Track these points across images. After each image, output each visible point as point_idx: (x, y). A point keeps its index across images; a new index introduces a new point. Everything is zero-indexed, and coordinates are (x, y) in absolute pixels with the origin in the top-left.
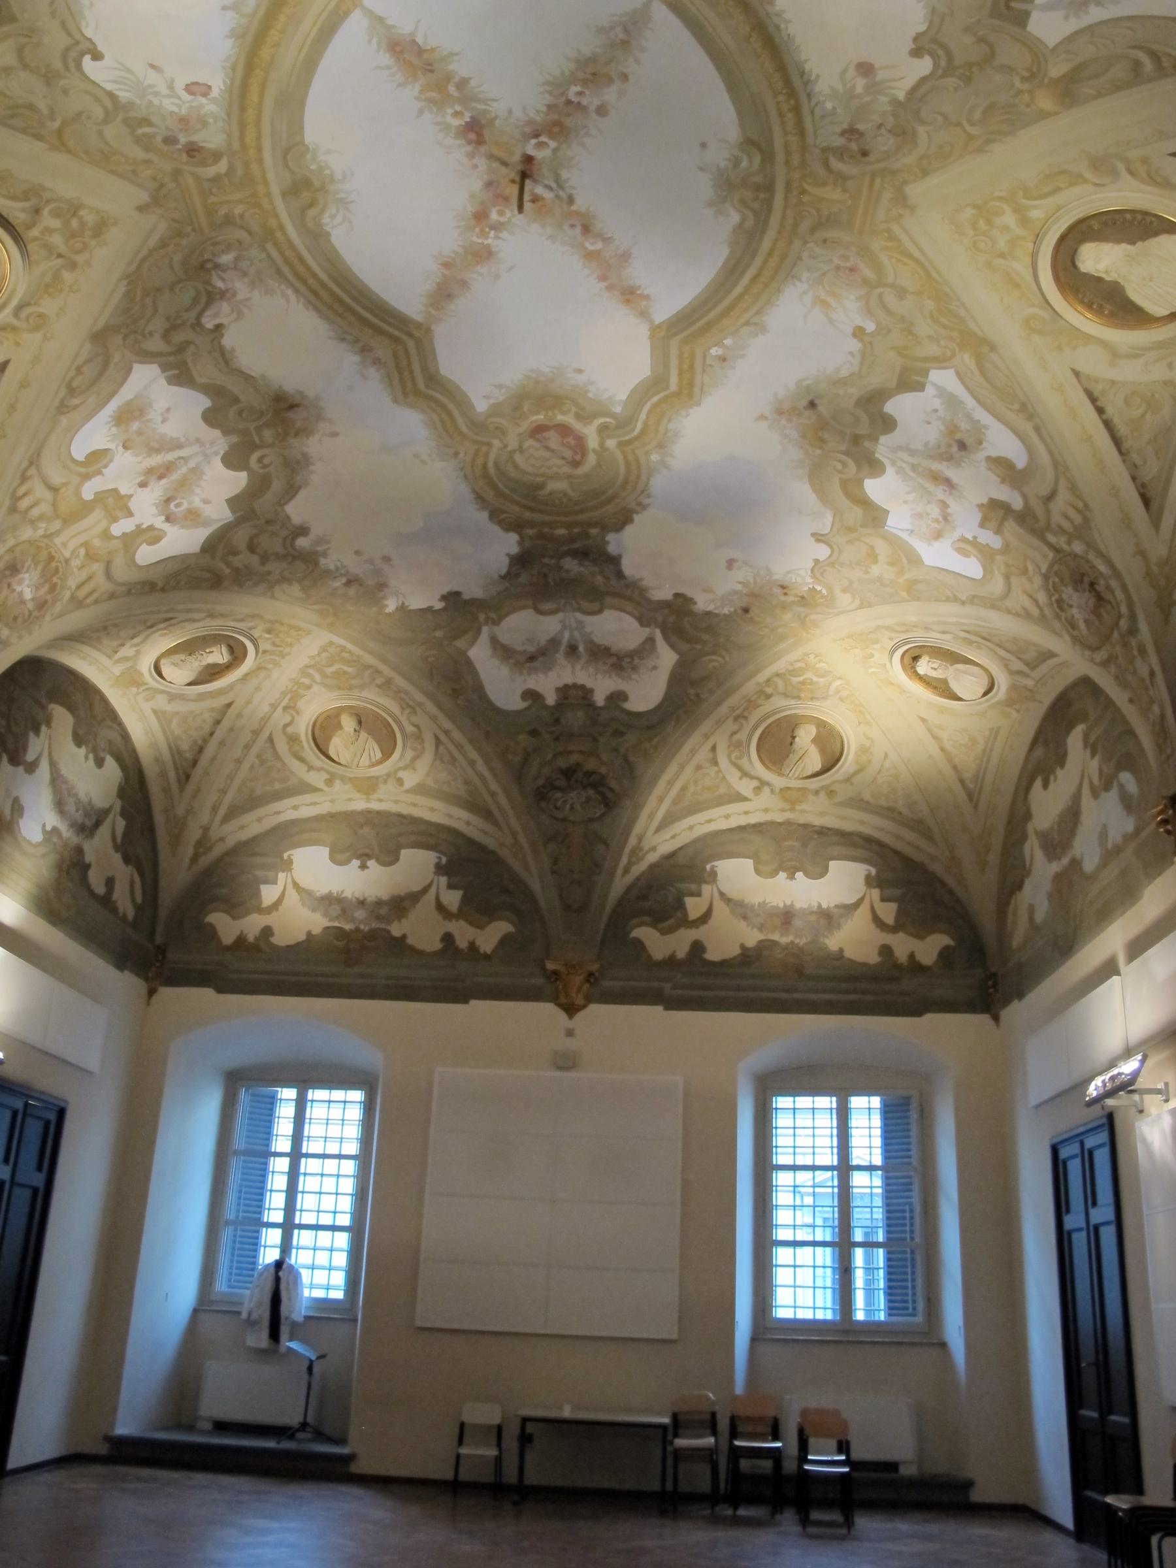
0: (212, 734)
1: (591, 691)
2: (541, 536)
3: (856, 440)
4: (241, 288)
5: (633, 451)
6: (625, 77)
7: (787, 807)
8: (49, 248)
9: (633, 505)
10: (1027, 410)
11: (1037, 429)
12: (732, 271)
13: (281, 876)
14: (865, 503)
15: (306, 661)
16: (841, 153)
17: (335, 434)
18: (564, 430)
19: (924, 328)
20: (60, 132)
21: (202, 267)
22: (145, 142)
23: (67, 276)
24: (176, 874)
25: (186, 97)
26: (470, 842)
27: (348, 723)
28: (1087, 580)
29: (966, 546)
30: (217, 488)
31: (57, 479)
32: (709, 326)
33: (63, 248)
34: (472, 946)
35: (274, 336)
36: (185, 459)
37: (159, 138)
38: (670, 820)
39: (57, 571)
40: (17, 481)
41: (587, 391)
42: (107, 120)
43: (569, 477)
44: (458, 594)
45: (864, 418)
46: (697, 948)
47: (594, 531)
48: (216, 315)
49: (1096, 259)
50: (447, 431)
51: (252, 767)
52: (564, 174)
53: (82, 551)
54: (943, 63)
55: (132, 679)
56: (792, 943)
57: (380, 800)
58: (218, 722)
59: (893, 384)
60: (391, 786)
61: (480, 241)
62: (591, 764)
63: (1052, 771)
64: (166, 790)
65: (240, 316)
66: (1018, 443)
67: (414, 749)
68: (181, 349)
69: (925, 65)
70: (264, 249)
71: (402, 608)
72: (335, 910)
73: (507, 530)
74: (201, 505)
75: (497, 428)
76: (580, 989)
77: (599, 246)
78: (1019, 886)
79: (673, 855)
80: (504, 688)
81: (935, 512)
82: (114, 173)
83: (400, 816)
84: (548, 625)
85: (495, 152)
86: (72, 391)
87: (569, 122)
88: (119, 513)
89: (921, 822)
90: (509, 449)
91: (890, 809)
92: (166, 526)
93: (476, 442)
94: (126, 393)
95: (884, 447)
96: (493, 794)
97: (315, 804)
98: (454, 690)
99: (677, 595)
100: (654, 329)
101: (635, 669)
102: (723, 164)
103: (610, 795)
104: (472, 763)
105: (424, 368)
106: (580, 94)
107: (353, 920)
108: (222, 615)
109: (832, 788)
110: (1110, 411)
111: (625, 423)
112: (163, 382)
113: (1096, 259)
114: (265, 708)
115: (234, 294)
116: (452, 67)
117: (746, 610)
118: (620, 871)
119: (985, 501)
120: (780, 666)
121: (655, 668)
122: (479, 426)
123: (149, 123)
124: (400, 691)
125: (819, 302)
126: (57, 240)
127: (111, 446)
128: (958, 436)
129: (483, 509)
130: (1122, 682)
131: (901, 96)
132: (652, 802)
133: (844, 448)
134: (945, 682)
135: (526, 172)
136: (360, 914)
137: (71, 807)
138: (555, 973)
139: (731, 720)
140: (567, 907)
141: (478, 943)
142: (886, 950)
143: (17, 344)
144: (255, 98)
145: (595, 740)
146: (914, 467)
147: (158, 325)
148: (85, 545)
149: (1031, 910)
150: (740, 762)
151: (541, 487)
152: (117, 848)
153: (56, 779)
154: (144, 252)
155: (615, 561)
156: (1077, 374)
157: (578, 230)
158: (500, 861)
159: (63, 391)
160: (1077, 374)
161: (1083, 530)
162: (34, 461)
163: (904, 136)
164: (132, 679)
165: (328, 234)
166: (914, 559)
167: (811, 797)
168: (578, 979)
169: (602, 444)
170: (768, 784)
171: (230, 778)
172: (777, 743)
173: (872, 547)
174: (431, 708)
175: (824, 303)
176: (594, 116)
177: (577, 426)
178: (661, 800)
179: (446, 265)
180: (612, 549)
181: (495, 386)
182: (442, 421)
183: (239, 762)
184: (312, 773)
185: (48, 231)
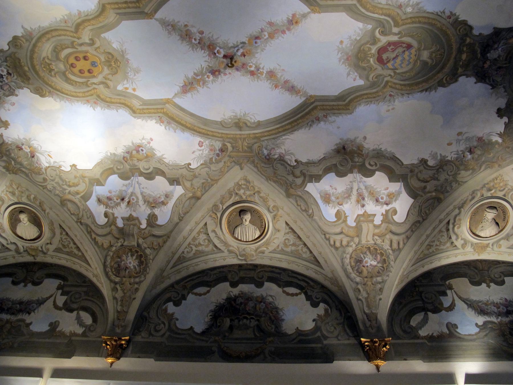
2: (466, 66)
5: (402, 20)
6: (186, 26)
8: (250, 196)
17: (365, 138)
18: (382, 50)
20: (212, 180)
21: (268, 159)
22: (217, 162)
25: (203, 148)
31: (338, 230)
33: (252, 192)
35: (305, 145)
39: (376, 249)
40: (327, 242)
41: (356, 39)
42: (210, 168)
47: (468, 40)
48: (290, 161)
50: (374, 97)
52: (231, 45)
61: (264, 75)
68: (304, 175)
70: (263, 141)
71: (500, 135)
73: (456, 81)
74: (388, 191)
75: (376, 78)
77: (266, 33)
82: (227, 172)
86: (306, 211)
87: (208, 43)
88: (371, 218)
90: (392, 74)
93: (385, 86)
100: (314, 11)
105: (333, 101)
106: (195, 40)
111: (380, 23)
112: (317, 184)
115: (282, 153)
116: (190, 77)
122: (373, 85)
123: (212, 158)
126: (248, 193)
143: (281, 217)
144: (204, 131)
147: (291, 178)
148: (374, 235)
154: (259, 173)
157: (258, 41)
165: (259, 121)
169: (396, 34)
176: (204, 35)
177: (379, 45)
179: (276, 87)
181: (348, 76)
182: (366, 98)
185: (244, 194)
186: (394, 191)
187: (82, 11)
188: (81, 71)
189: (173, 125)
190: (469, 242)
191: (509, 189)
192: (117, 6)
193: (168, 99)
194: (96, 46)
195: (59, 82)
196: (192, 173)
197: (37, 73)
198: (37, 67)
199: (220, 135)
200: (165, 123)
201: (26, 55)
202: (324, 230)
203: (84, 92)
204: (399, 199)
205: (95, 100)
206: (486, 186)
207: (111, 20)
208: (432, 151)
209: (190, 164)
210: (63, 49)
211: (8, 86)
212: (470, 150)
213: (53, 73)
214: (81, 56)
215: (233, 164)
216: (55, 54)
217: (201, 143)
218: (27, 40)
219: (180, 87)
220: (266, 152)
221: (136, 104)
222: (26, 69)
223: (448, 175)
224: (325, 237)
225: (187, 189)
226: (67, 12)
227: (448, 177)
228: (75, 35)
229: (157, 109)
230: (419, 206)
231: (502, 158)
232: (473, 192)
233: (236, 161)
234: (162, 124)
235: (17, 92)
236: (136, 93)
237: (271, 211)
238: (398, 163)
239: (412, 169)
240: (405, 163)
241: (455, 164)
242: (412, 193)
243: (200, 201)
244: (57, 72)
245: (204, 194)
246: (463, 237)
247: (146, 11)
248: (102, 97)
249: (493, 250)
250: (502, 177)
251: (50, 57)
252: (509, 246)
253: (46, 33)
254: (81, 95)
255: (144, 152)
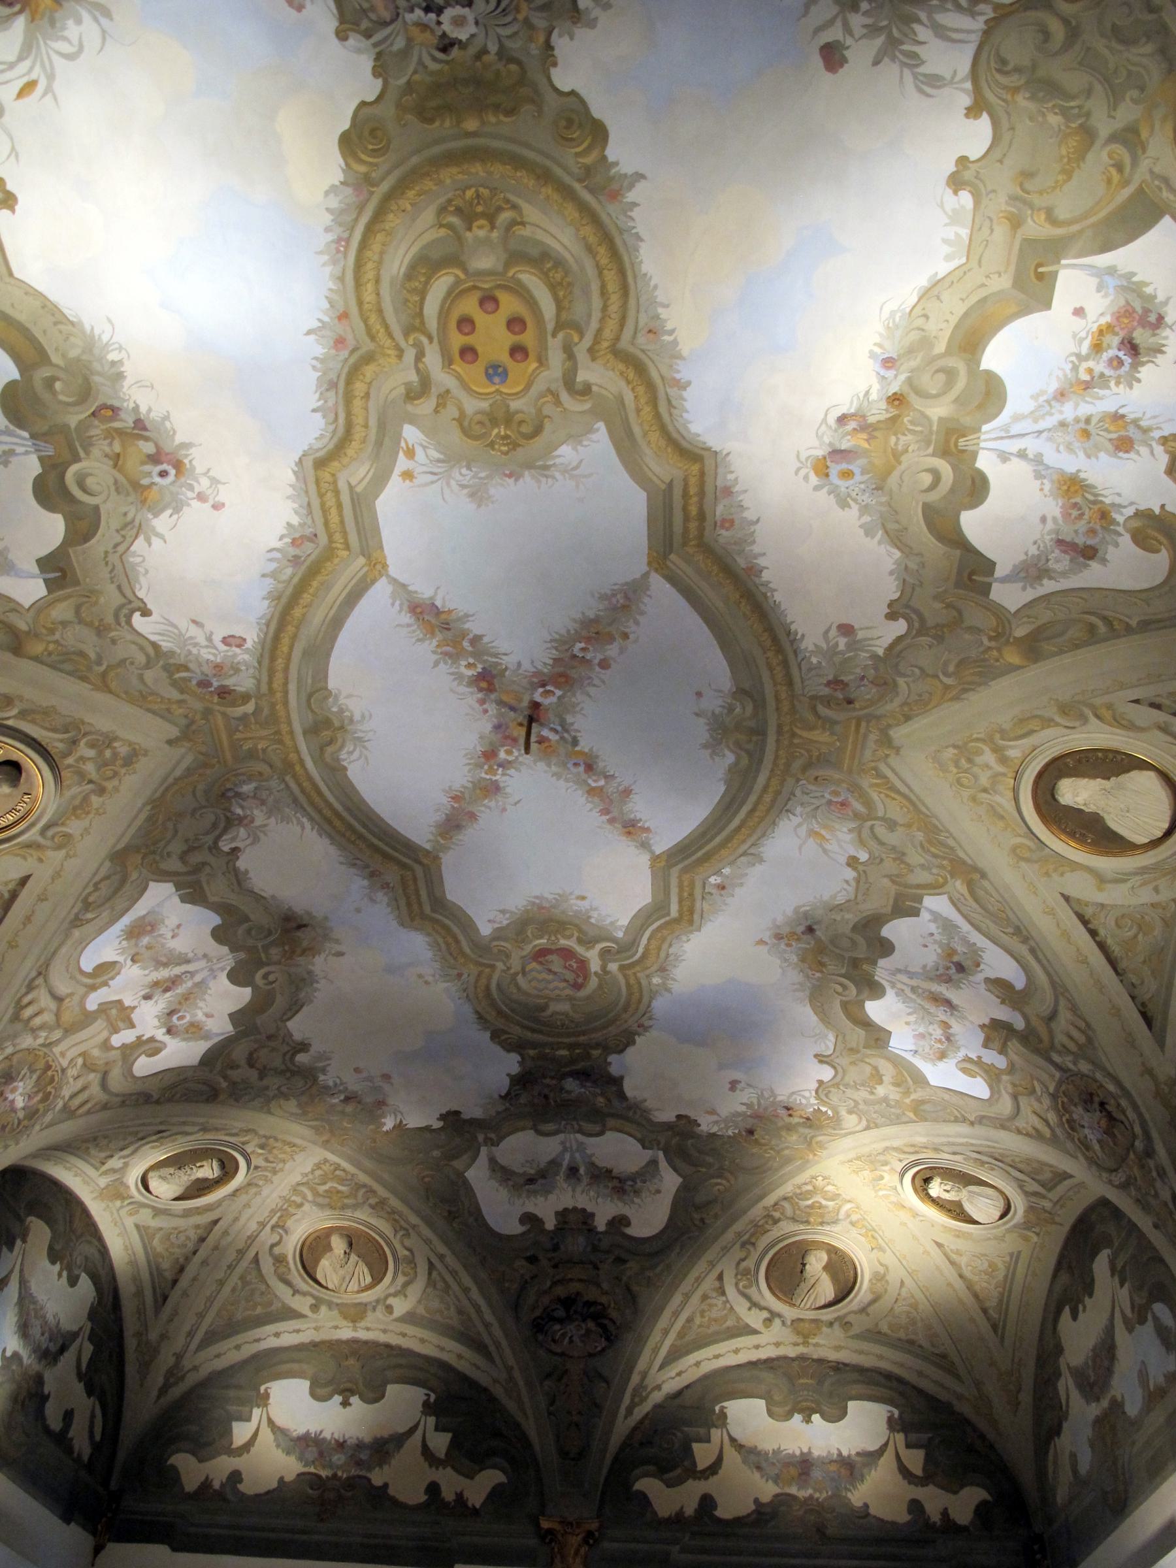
0: (195, 1253)
1: (592, 1215)
3: (855, 963)
4: (259, 817)
7: (800, 1340)
8: (81, 775)
9: (635, 1027)
10: (1021, 933)
11: (1032, 951)
12: (727, 807)
13: (256, 1412)
14: (867, 1024)
15: (298, 1178)
16: (828, 701)
17: (340, 954)
18: (567, 953)
19: (915, 857)
20: (104, 675)
21: (223, 795)
23: (95, 800)
24: (142, 1407)
25: (222, 647)
26: (464, 1378)
27: (338, 1245)
28: (1096, 1099)
29: (971, 1066)
30: (220, 1003)
31: (62, 989)
32: (707, 858)
34: (460, 1496)
36: (192, 974)
37: (194, 682)
38: (675, 1354)
39: (52, 1079)
40: (24, 990)
42: (148, 665)
43: (570, 999)
44: (457, 1113)
45: (860, 940)
46: (707, 1503)
47: (595, 1053)
48: (233, 839)
49: (1076, 792)
51: (234, 1290)
52: (569, 719)
53: (80, 1061)
54: (917, 625)
55: (117, 1192)
56: (811, 1497)
57: (368, 1329)
58: (202, 1240)
59: (889, 909)
60: (380, 1313)
62: (591, 1294)
63: (1080, 1301)
64: (141, 1312)
65: (256, 840)
66: (1015, 964)
67: (405, 1274)
68: (197, 869)
69: (900, 627)
71: (399, 1126)
72: (312, 1453)
73: (508, 1051)
76: (577, 1553)
77: (602, 783)
78: (1056, 1431)
79: (679, 1393)
80: (502, 1210)
81: (938, 1032)
82: (148, 710)
83: (388, 1346)
84: (548, 1147)
85: (505, 698)
86: (87, 906)
87: (573, 673)
88: (121, 1024)
89: (944, 1356)
91: (911, 1342)
92: (167, 1039)
94: (140, 909)
95: (882, 970)
96: (487, 1326)
97: (298, 1331)
98: (450, 1212)
99: (679, 1117)
100: (655, 859)
101: (637, 1192)
102: (718, 711)
103: (611, 1328)
104: (466, 1290)
105: (431, 894)
106: (583, 649)
107: (331, 1466)
108: (217, 1129)
109: (848, 1319)
110: (1102, 932)
111: (626, 947)
112: (176, 900)
113: (1076, 792)
114: (253, 1226)
115: (252, 821)
116: (466, 626)
117: (751, 1132)
118: (622, 1411)
119: (987, 1021)
120: (788, 1189)
121: (658, 1191)
122: (482, 948)
123: (187, 669)
124: (394, 1213)
125: (812, 833)
126: (90, 768)
127: (120, 959)
128: (956, 959)
129: (485, 1029)
130: (1142, 1204)
131: (880, 652)
132: (655, 1337)
133: (843, 971)
134: (959, 1204)
135: (533, 716)
136: (338, 1458)
137: (36, 1331)
138: (550, 1531)
139: (738, 1246)
140: (563, 1454)
141: (466, 1494)
142: (915, 1506)
143: (40, 860)
145: (596, 1268)
146: (914, 989)
147: (177, 847)
148: (83, 1054)
149: (1073, 1456)
150: (749, 1291)
151: (544, 1008)
152: (80, 1376)
153: (25, 1300)
154: (171, 780)
155: (617, 1082)
156: (1067, 899)
157: (582, 769)
158: (492, 1399)
159: (79, 905)
160: (1067, 899)
161: (1087, 1048)
162: (42, 972)
163: (886, 686)
164: (117, 1192)
165: (345, 769)
166: (920, 1080)
167: (825, 1329)
168: (575, 1540)
169: (604, 968)
170: (779, 1315)
171: (210, 1300)
172: (787, 1272)
173: (876, 1068)
174: (427, 1232)
175: (817, 834)
176: (597, 669)
177: (580, 949)
178: (666, 1332)
180: (614, 1070)
182: (447, 944)
183: (221, 1283)
184: (297, 1297)
187: (685, 394)
188: (466, 324)
189: (289, 571)
192: (693, 490)
193: (385, 566)
194: (564, 396)
195: (413, 233)
196: (110, 619)
197: (450, 159)
198: (478, 169)
199: (276, 685)
200: (292, 551)
201: (527, 146)
202: (51, 967)
203: (380, 311)
205: (351, 342)
207: (653, 464)
209: (146, 613)
210: (553, 287)
211: (387, 15)
213: (454, 220)
214: (528, 338)
215: (184, 722)
216: (535, 252)
217: (238, 642)
218: (588, 171)
219: (431, 598)
220: (246, 788)
221: (355, 473)
222: (471, 125)
224: (33, 979)
225: (39, 611)
226: (685, 349)
228: (605, 344)
229: (345, 533)
233: (194, 727)
234: (288, 540)
235: (354, 40)
236: (395, 481)
237: (50, 833)
243: (8, 657)
244: (459, 239)
245: (42, 663)
247: (673, 557)
248: (369, 370)
251: (520, 231)
253: (613, 250)
254: (369, 297)
255: (157, 479)
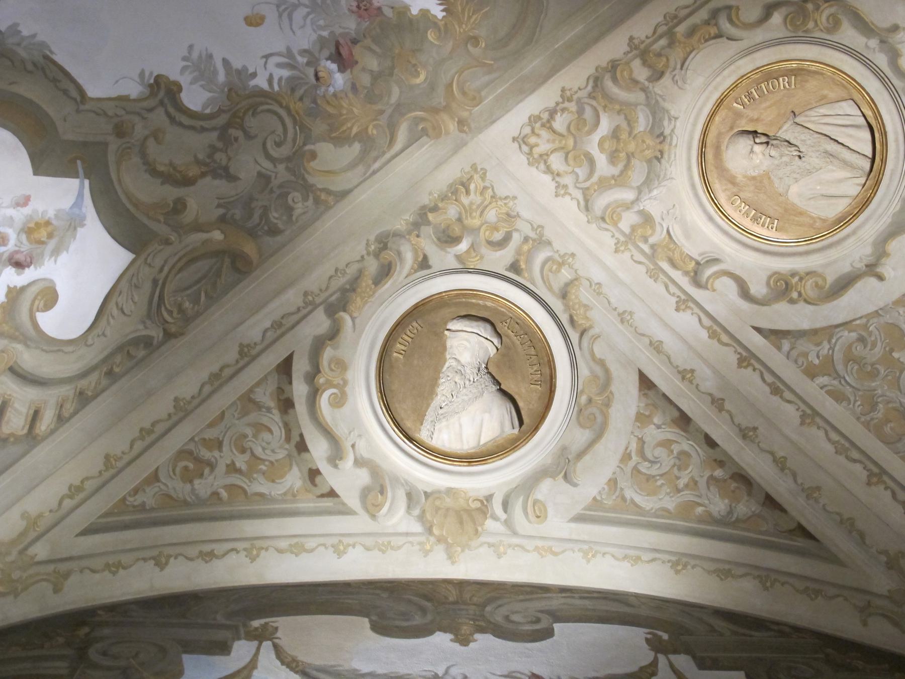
0: (711, 443)
51: (838, 397)
58: (683, 420)
64: (813, 589)
67: (835, 25)
74: (27, 210)
124: (670, 34)
171: (846, 447)
183: (811, 416)
184: (886, 269)
186: (51, 214)
190: (396, 480)
191: (526, 239)
204: (73, 247)
206: (431, 216)
208: (191, 47)
212: (339, 54)
223: (268, 157)
227: (267, 164)
230: (155, 282)
231: (464, 94)
232: (384, 243)
238: (65, 92)
239: (120, 117)
240: (93, 91)
241: (288, 109)
242: (127, 225)
246: (363, 449)
249: (515, 533)
250: (483, 178)
252: (578, 510)
